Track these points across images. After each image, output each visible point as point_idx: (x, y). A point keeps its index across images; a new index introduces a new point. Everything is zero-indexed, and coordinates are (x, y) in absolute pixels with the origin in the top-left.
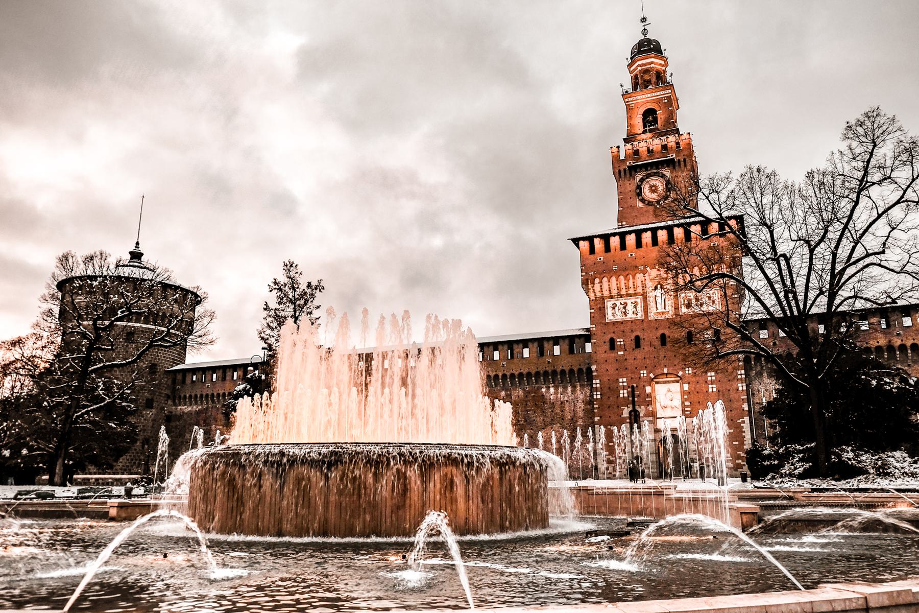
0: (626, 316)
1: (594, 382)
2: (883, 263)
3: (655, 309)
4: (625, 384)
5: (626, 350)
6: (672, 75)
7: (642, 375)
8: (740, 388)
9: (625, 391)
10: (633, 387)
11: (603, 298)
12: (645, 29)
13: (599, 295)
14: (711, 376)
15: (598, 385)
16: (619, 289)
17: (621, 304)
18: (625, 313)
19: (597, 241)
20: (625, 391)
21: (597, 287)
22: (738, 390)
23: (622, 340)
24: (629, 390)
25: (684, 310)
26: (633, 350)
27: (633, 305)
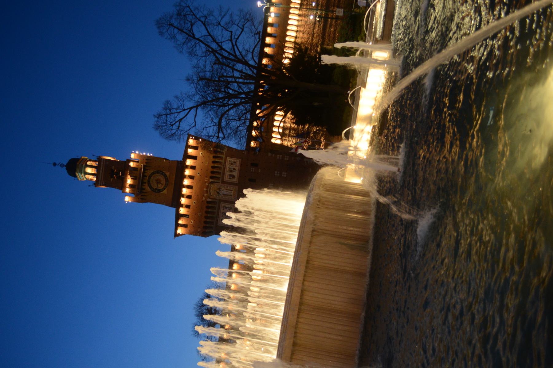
2: (236, 37)
3: (231, 197)
6: (94, 155)
8: (287, 159)
12: (60, 165)
17: (222, 216)
19: (180, 222)
25: (235, 180)
27: (225, 209)
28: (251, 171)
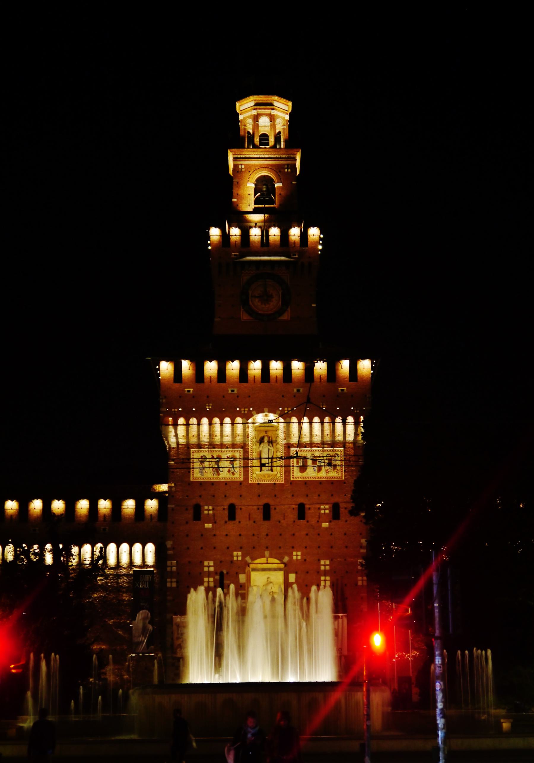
0: (219, 474)
1: (169, 563)
4: (212, 569)
5: (215, 522)
7: (235, 558)
8: (360, 583)
9: (211, 579)
10: (222, 574)
11: (188, 446)
13: (182, 441)
14: (325, 565)
15: (174, 569)
16: (211, 435)
17: (213, 457)
18: (217, 470)
20: (211, 579)
21: (181, 430)
22: (356, 584)
23: (211, 508)
24: (218, 577)
25: (296, 474)
26: (226, 522)
28: (322, 507)
